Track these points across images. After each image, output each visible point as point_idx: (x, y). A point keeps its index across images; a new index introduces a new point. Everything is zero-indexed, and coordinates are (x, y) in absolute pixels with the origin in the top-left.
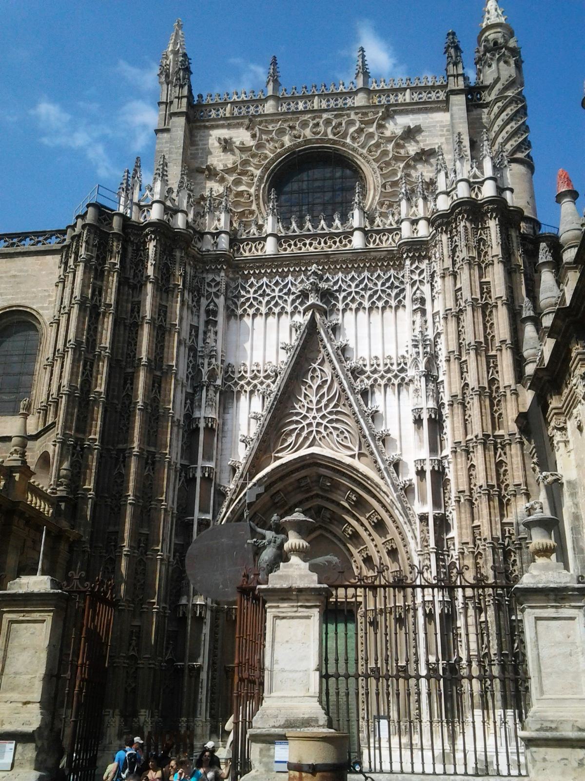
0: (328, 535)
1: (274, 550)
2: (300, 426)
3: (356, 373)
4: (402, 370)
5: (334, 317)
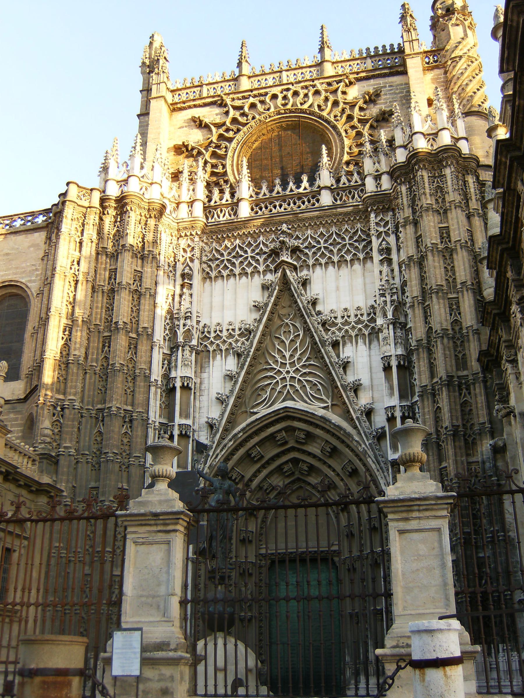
2: (275, 381)
3: (326, 326)
4: (373, 320)
5: (305, 272)
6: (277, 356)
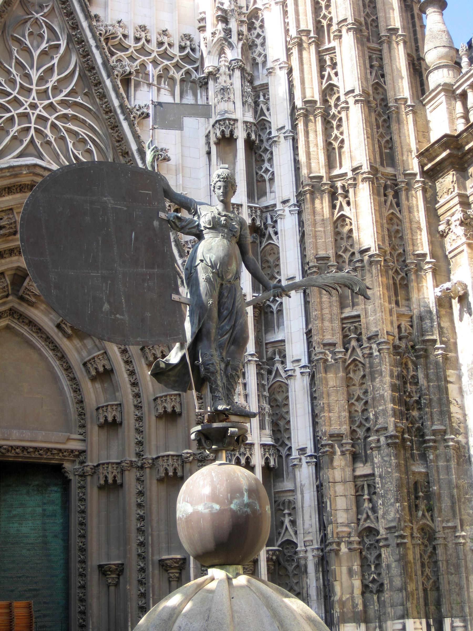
0: (24, 330)
2: (8, 115)
6: (13, 70)
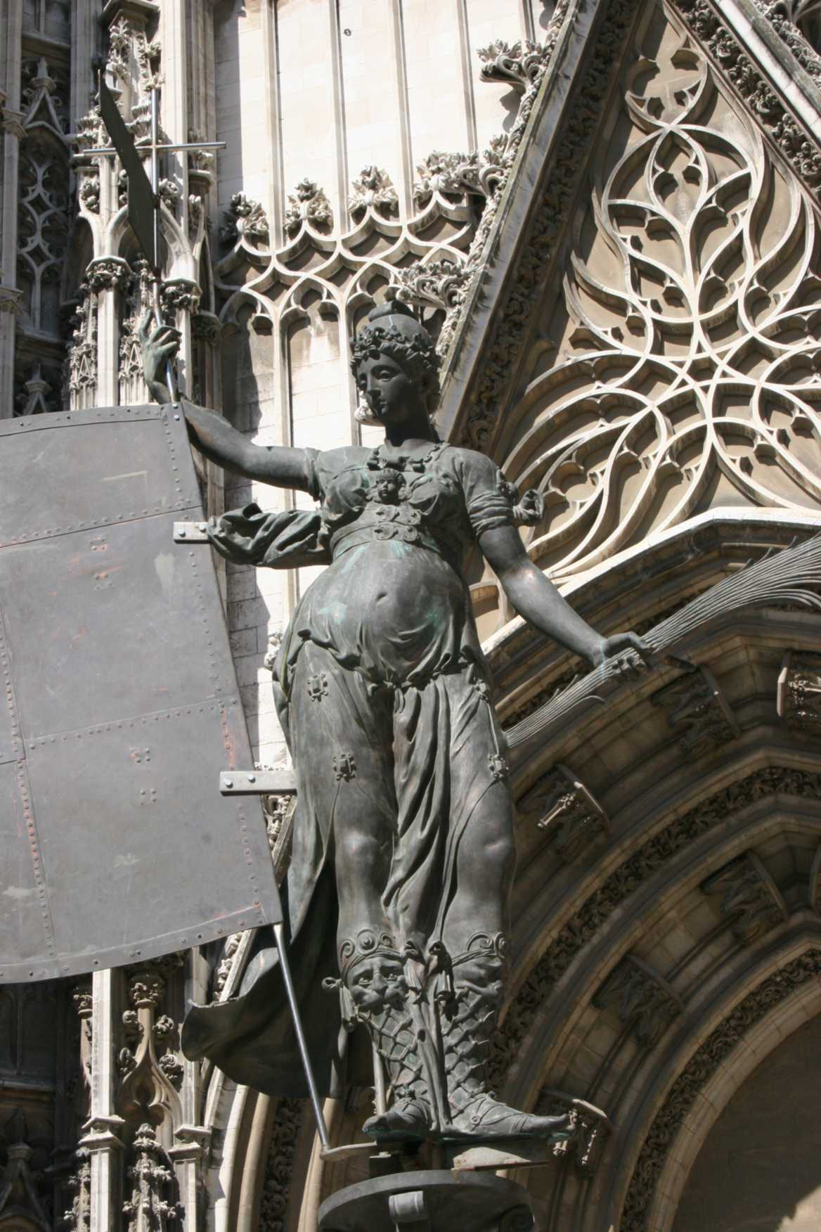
1: (397, 547)
6: (631, 297)
